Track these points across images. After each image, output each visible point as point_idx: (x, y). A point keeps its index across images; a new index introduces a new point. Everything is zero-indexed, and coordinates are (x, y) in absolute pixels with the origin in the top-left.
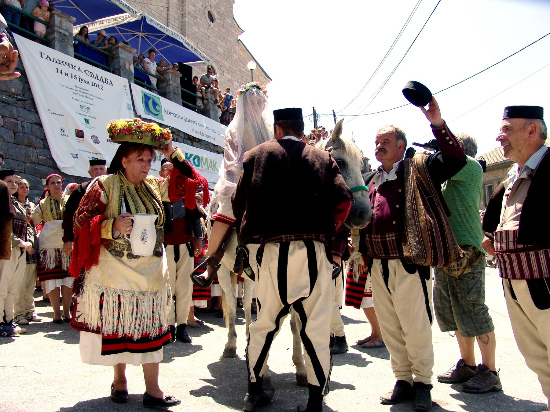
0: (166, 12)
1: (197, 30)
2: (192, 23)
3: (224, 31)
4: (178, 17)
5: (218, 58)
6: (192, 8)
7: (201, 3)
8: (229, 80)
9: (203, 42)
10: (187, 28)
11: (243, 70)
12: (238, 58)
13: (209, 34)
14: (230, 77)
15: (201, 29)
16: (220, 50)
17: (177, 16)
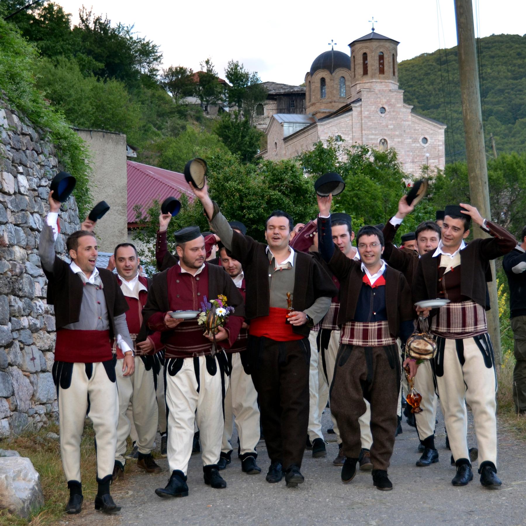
0: (351, 122)
1: (371, 124)
2: (367, 121)
3: (394, 113)
4: (358, 121)
5: (389, 133)
6: (366, 113)
7: (374, 107)
8: (399, 142)
9: (376, 128)
10: (363, 126)
11: (417, 128)
12: (410, 123)
13: (381, 122)
14: (400, 140)
15: (374, 122)
16: (392, 127)
17: (358, 121)
